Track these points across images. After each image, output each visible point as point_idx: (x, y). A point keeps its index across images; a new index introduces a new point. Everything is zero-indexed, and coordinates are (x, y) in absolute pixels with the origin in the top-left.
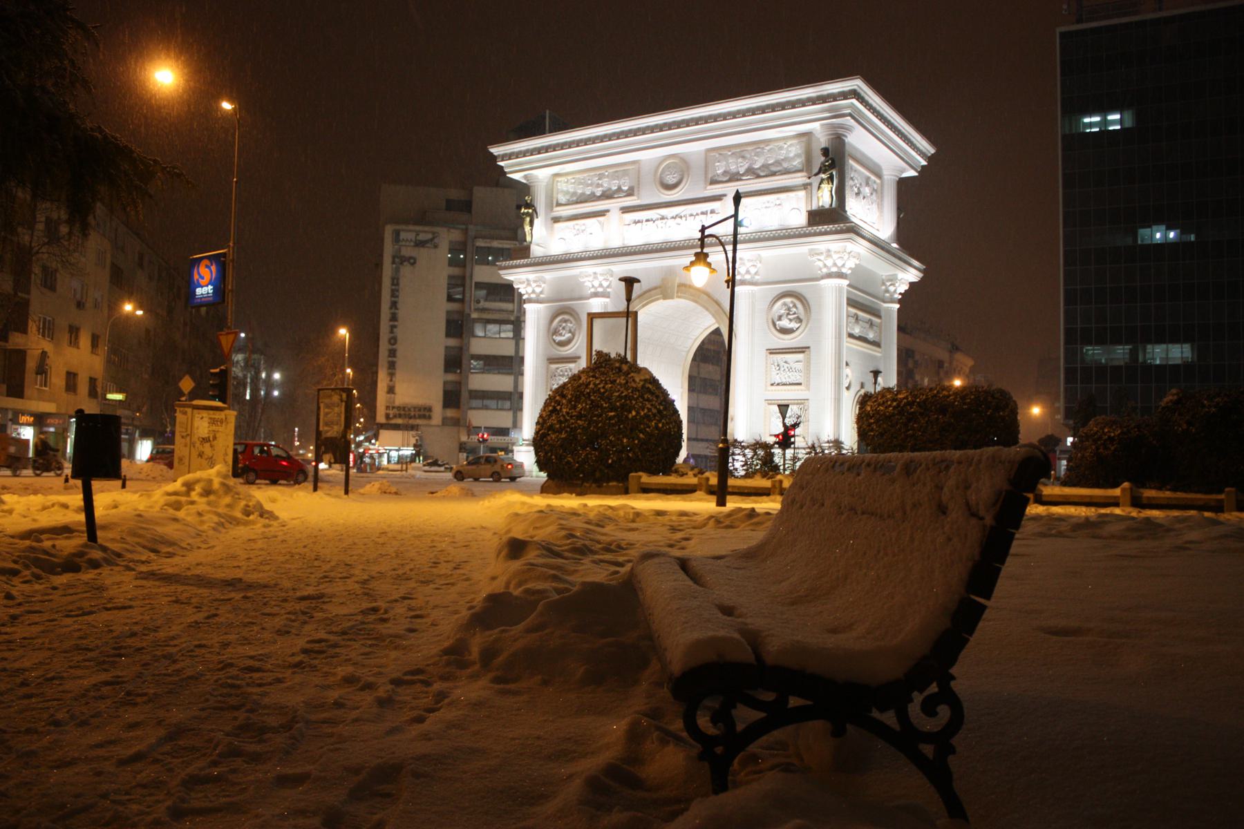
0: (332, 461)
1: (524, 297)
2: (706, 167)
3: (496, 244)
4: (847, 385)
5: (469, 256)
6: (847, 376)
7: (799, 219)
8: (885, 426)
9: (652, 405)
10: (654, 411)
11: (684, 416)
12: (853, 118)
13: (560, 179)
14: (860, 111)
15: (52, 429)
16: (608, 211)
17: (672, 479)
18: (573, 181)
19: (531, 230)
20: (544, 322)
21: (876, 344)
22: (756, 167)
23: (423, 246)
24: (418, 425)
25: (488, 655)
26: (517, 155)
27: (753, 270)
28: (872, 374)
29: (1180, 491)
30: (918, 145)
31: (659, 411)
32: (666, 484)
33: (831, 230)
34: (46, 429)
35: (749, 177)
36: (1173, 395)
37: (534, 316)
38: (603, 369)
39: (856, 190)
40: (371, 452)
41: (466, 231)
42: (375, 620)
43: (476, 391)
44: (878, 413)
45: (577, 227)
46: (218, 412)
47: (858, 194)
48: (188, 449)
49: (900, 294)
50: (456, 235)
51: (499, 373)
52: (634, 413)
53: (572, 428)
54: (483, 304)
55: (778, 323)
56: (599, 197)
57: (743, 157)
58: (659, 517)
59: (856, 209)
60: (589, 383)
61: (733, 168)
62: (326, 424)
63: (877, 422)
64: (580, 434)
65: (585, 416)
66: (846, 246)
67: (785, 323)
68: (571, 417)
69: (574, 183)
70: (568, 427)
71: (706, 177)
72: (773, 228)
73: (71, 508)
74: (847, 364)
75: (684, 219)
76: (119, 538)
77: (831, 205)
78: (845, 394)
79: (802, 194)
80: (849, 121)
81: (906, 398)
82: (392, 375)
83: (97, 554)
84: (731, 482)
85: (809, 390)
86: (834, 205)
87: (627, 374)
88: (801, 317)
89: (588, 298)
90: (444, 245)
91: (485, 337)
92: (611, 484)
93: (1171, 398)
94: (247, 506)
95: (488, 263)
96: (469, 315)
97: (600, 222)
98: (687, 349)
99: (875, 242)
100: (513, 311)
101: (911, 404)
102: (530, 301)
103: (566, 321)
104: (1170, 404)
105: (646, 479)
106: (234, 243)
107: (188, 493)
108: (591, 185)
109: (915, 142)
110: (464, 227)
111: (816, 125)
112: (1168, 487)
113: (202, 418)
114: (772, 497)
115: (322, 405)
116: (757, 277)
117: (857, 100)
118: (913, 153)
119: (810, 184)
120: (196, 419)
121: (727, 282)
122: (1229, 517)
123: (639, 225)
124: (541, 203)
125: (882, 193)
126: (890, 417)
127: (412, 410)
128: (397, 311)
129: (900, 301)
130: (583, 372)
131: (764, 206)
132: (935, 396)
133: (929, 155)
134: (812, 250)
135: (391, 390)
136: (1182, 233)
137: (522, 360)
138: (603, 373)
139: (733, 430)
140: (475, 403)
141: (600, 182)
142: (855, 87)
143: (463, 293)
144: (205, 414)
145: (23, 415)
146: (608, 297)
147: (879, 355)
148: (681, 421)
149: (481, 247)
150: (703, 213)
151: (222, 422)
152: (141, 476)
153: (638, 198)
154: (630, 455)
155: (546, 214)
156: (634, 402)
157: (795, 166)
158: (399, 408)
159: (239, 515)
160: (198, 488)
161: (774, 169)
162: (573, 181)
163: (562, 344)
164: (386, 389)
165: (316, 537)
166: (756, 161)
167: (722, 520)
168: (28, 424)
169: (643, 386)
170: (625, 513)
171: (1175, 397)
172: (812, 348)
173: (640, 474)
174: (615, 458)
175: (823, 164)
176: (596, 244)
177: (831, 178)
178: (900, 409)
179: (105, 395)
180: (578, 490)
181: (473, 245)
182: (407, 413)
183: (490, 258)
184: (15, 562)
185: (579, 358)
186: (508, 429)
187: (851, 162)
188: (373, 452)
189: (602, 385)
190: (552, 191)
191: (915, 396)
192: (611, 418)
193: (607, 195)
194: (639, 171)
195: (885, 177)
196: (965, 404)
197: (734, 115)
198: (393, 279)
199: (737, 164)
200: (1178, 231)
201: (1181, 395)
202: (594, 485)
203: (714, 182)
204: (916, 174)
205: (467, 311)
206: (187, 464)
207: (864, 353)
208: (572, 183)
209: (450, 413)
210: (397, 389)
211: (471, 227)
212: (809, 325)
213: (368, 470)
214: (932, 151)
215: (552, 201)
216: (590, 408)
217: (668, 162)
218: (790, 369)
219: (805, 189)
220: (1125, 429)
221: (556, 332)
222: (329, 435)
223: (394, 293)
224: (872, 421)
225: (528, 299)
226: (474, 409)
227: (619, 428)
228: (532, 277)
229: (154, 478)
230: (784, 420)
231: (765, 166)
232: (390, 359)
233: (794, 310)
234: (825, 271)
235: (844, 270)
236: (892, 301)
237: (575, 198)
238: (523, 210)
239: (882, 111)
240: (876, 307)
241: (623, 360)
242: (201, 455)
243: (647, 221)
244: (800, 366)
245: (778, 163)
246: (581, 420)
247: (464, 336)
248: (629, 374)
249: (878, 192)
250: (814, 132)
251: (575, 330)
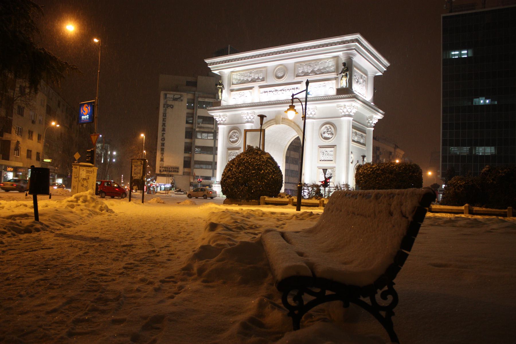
0: (137, 189)
1: (218, 122)
3: (207, 100)
4: (351, 161)
5: (195, 105)
6: (352, 157)
7: (333, 92)
8: (367, 179)
9: (270, 168)
10: (271, 171)
11: (283, 173)
12: (356, 50)
13: (234, 74)
14: (359, 48)
15: (21, 174)
16: (253, 87)
17: (278, 199)
18: (239, 74)
19: (222, 94)
20: (226, 133)
21: (364, 144)
22: (315, 70)
23: (176, 100)
24: (173, 175)
25: (201, 271)
26: (216, 63)
27: (313, 113)
28: (362, 157)
29: (489, 208)
30: (383, 62)
31: (273, 171)
32: (276, 201)
33: (346, 97)
34: (18, 173)
35: (312, 74)
36: (487, 168)
37: (222, 130)
38: (250, 153)
39: (357, 80)
40: (153, 185)
41: (194, 94)
42: (154, 255)
43: (197, 161)
44: (364, 173)
45: (240, 94)
46: (90, 168)
47: (357, 82)
48: (77, 183)
49: (374, 124)
50: (190, 96)
51: (207, 154)
52: (263, 171)
53: (237, 177)
54: (201, 125)
55: (323, 135)
56: (250, 81)
57: (310, 66)
58: (273, 215)
59: (357, 88)
60: (244, 159)
61: (306, 70)
62: (135, 174)
63: (364, 177)
64: (240, 179)
65: (243, 172)
66: (352, 104)
67: (326, 135)
68: (237, 172)
69: (240, 75)
70: (235, 177)
71: (294, 74)
72: (322, 96)
73: (28, 206)
74: (352, 153)
75: (285, 91)
76: (48, 219)
77: (346, 86)
78: (351, 165)
79: (334, 81)
80: (354, 52)
81: (376, 167)
82: (162, 154)
83: (39, 226)
84: (303, 201)
85: (335, 162)
86: (347, 87)
87: (260, 155)
88: (333, 133)
89: (244, 123)
90: (185, 100)
91: (201, 138)
92: (253, 201)
93: (486, 169)
94: (101, 207)
95: (203, 108)
96: (195, 129)
97: (250, 92)
98: (285, 145)
99: (364, 102)
100: (213, 128)
101: (378, 170)
102: (220, 124)
103: (235, 133)
104: (486, 172)
105: (267, 199)
106: (98, 98)
107: (77, 201)
108: (247, 76)
109: (382, 61)
110: (194, 93)
111: (340, 54)
112: (484, 206)
113: (83, 170)
114: (319, 207)
115: (133, 166)
116: (315, 116)
117: (358, 43)
118: (381, 65)
119: (338, 78)
120: (81, 170)
121: (303, 117)
122: (509, 219)
123: (266, 93)
124: (226, 84)
125: (367, 82)
126: (369, 175)
127: (171, 168)
128: (165, 127)
129: (374, 127)
130: (242, 154)
131: (318, 86)
132: (388, 166)
133: (388, 66)
134: (337, 105)
135: (162, 160)
136: (492, 101)
137: (217, 148)
138: (250, 155)
139: (304, 179)
140: (196, 166)
141: (251, 75)
142: (357, 38)
143: (193, 120)
144: (84, 168)
145: (9, 167)
146: (253, 123)
147: (365, 149)
148: (282, 175)
149: (201, 101)
150: (293, 89)
151: (91, 172)
152: (58, 194)
154: (261, 189)
155: (228, 89)
156: (263, 167)
157: (331, 70)
158: (165, 167)
159: (98, 211)
160: (81, 199)
161: (323, 71)
162: (239, 74)
163: (233, 142)
164: (160, 159)
165: (130, 220)
166: (315, 67)
167: (299, 216)
168: (11, 171)
169: (267, 160)
170: (258, 213)
171: (488, 169)
172: (337, 146)
173: (265, 197)
174: (254, 190)
175: (343, 69)
176: (249, 101)
177: (346, 75)
178: (373, 172)
179: (43, 160)
180: (239, 203)
181: (197, 100)
182: (169, 169)
183: (204, 106)
184: (5, 228)
185: (240, 148)
186: (210, 177)
187: (355, 69)
188: (154, 185)
189: (250, 160)
190: (231, 78)
191: (380, 167)
192: (253, 173)
193: (253, 81)
194: (267, 71)
195: (369, 75)
196: (400, 170)
197: (306, 48)
198: (164, 114)
199: (307, 69)
200: (490, 100)
201: (490, 168)
202: (246, 201)
203: (297, 76)
204: (381, 74)
205: (194, 128)
206: (77, 189)
207: (358, 148)
208: (239, 75)
209: (186, 170)
210: (165, 159)
211: (196, 93)
212: (336, 136)
213: (152, 193)
214: (389, 65)
215: (230, 83)
216: (245, 169)
217: (279, 67)
218: (328, 154)
219: (336, 79)
220: (467, 182)
221: (231, 137)
222: (136, 178)
223: (164, 120)
224: (362, 176)
225: (219, 123)
226: (197, 168)
227: (257, 178)
228: (221, 114)
229: (63, 195)
230: (325, 176)
231: (319, 70)
232: (162, 147)
233: (330, 130)
234: (343, 113)
235: (351, 114)
236: (371, 127)
237: (240, 82)
238: (218, 86)
239: (368, 48)
240: (364, 129)
241: (259, 149)
242: (82, 185)
243: (270, 91)
244: (332, 153)
245: (324, 68)
246: (241, 174)
247: (193, 138)
248: (261, 155)
249: (366, 81)
250: (340, 56)
251: (239, 136)
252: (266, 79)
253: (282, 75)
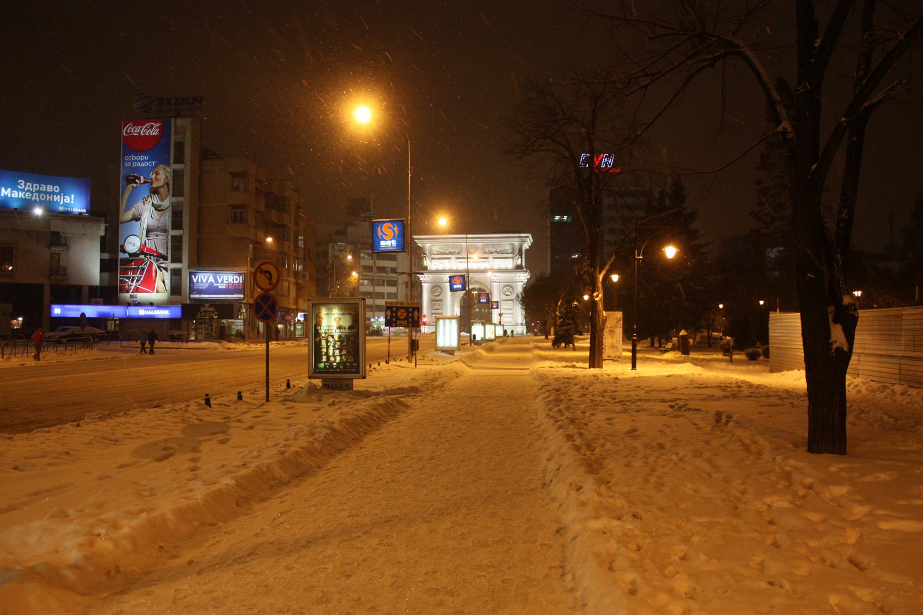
37: (426, 288)
57: (494, 247)
61: (491, 250)
67: (507, 293)
79: (511, 259)
85: (514, 310)
102: (425, 282)
124: (427, 252)
193: (450, 253)
194: (461, 248)
203: (485, 253)
221: (434, 292)
231: (500, 251)
244: (511, 304)
245: (504, 250)
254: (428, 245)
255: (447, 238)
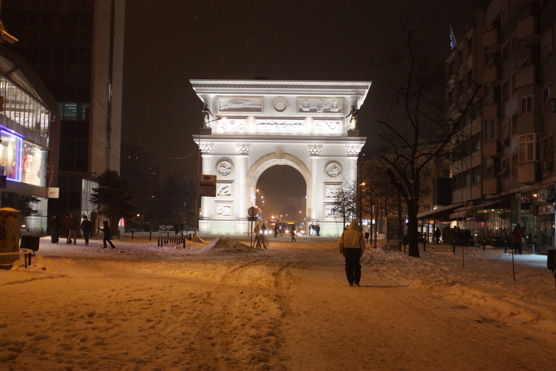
1: (202, 151)
2: (297, 104)
16: (248, 117)
26: (201, 85)
27: (319, 150)
71: (297, 109)
75: (287, 125)
102: (206, 153)
111: (349, 96)
124: (211, 108)
150: (295, 124)
153: (264, 113)
185: (233, 181)
194: (263, 102)
203: (301, 111)
219: (342, 120)
234: (351, 153)
252: (264, 110)
253: (283, 108)
254: (212, 96)
255: (244, 86)
